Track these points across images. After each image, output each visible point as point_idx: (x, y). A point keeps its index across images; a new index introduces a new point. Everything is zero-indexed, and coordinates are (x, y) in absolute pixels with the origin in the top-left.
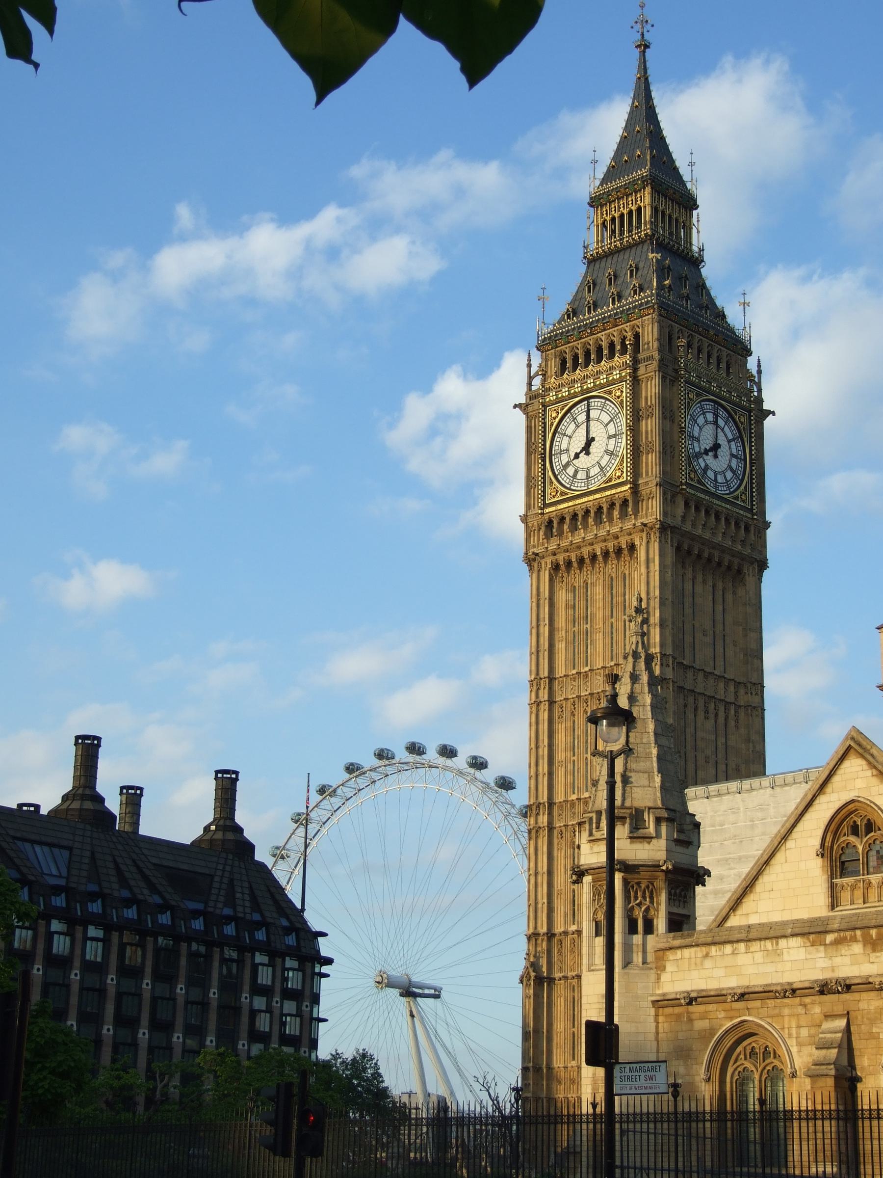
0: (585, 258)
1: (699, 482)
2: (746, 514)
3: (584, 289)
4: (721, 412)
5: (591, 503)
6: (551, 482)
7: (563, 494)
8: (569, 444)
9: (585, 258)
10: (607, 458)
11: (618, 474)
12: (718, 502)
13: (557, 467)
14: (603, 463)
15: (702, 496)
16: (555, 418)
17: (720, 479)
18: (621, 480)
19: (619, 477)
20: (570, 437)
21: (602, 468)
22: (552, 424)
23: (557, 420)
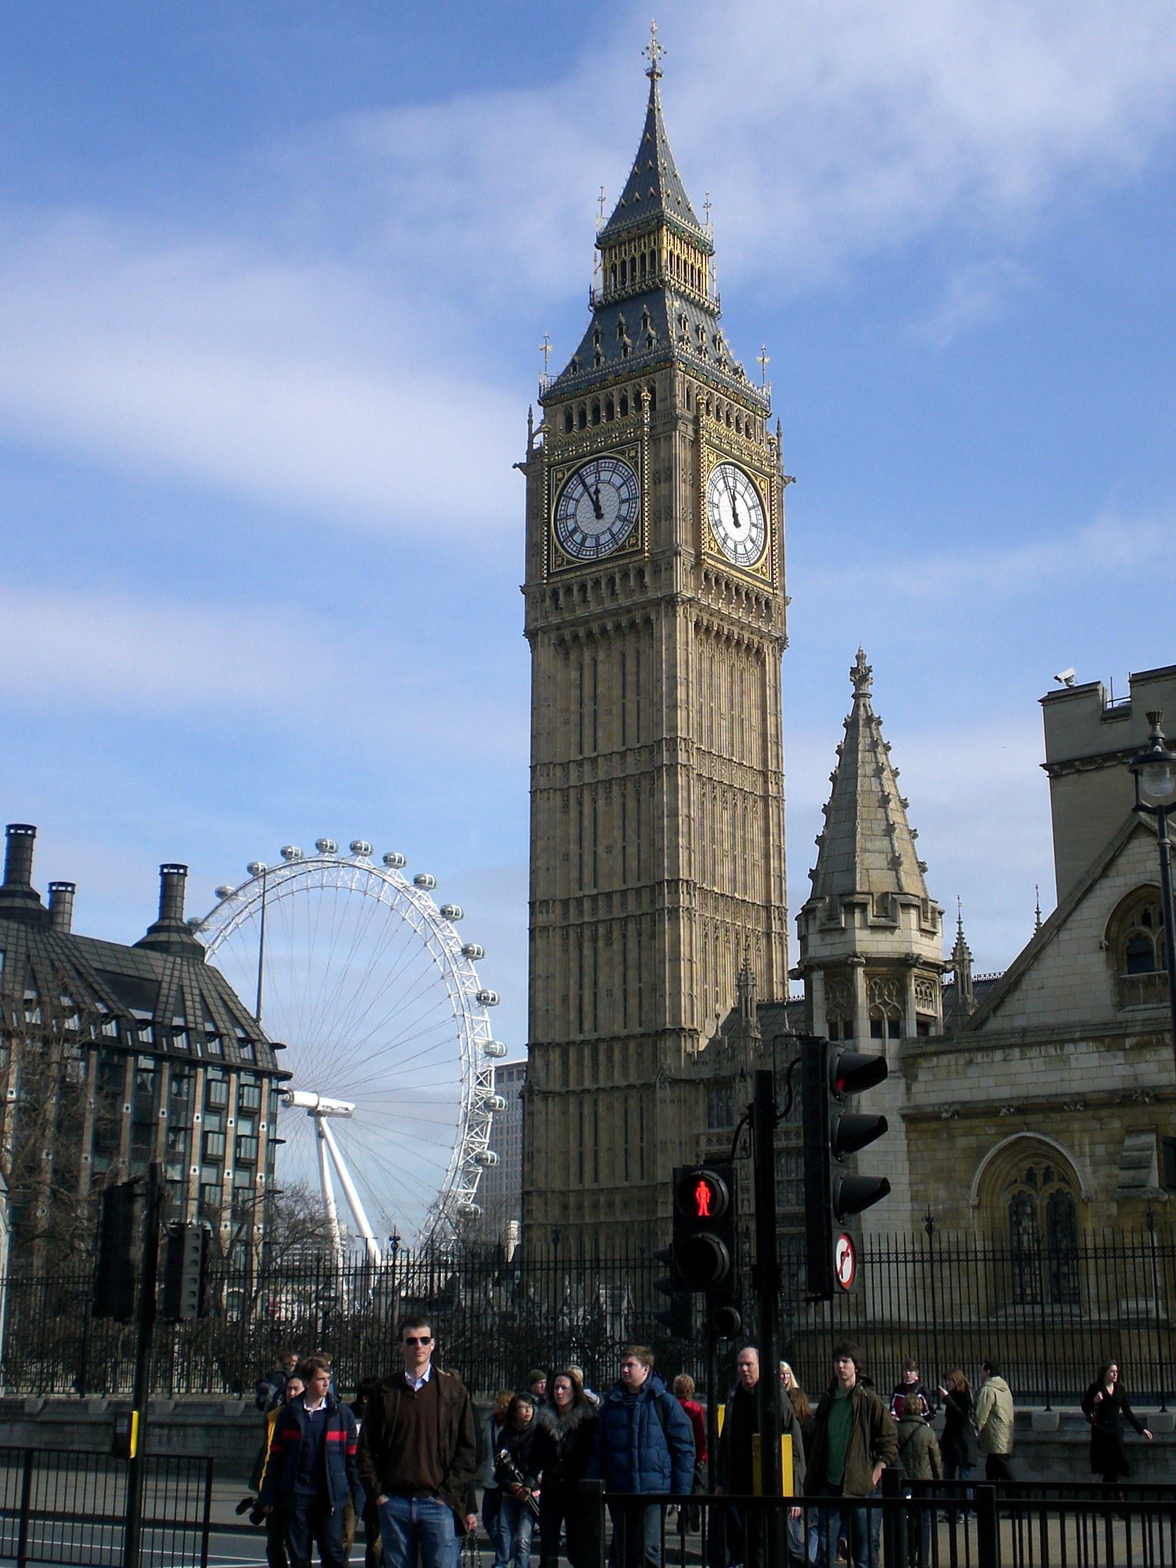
0: (591, 305)
1: (719, 552)
2: (766, 588)
3: (592, 340)
4: (740, 475)
5: (602, 573)
6: (557, 550)
7: (569, 562)
8: (576, 508)
9: (591, 305)
10: (619, 524)
11: (633, 541)
12: (739, 575)
13: (563, 534)
14: (615, 530)
15: (723, 567)
16: (560, 480)
17: (740, 549)
18: (635, 549)
19: (633, 546)
20: (578, 501)
21: (613, 536)
22: (557, 486)
23: (563, 481)
